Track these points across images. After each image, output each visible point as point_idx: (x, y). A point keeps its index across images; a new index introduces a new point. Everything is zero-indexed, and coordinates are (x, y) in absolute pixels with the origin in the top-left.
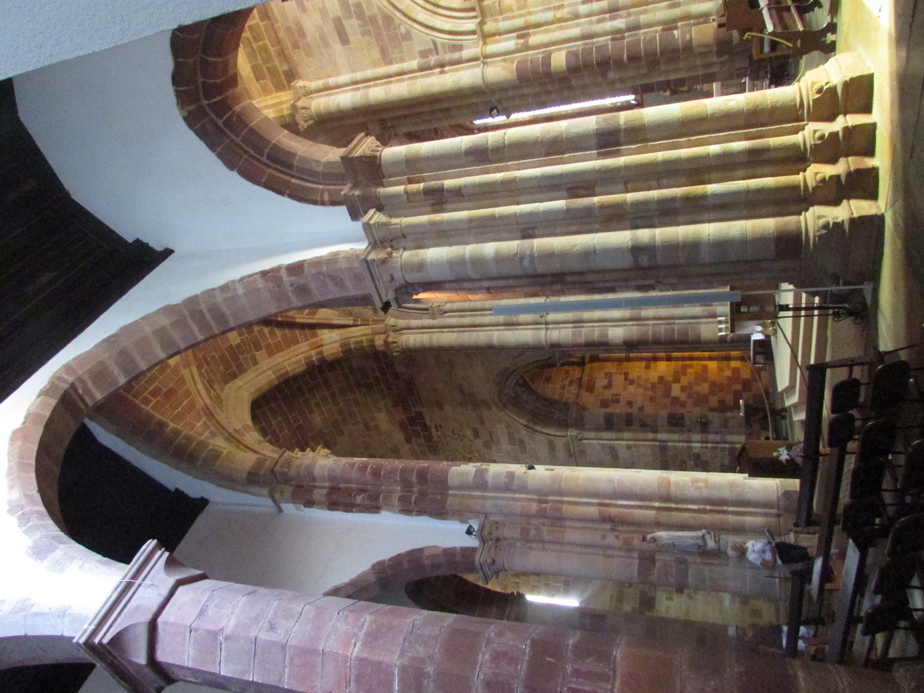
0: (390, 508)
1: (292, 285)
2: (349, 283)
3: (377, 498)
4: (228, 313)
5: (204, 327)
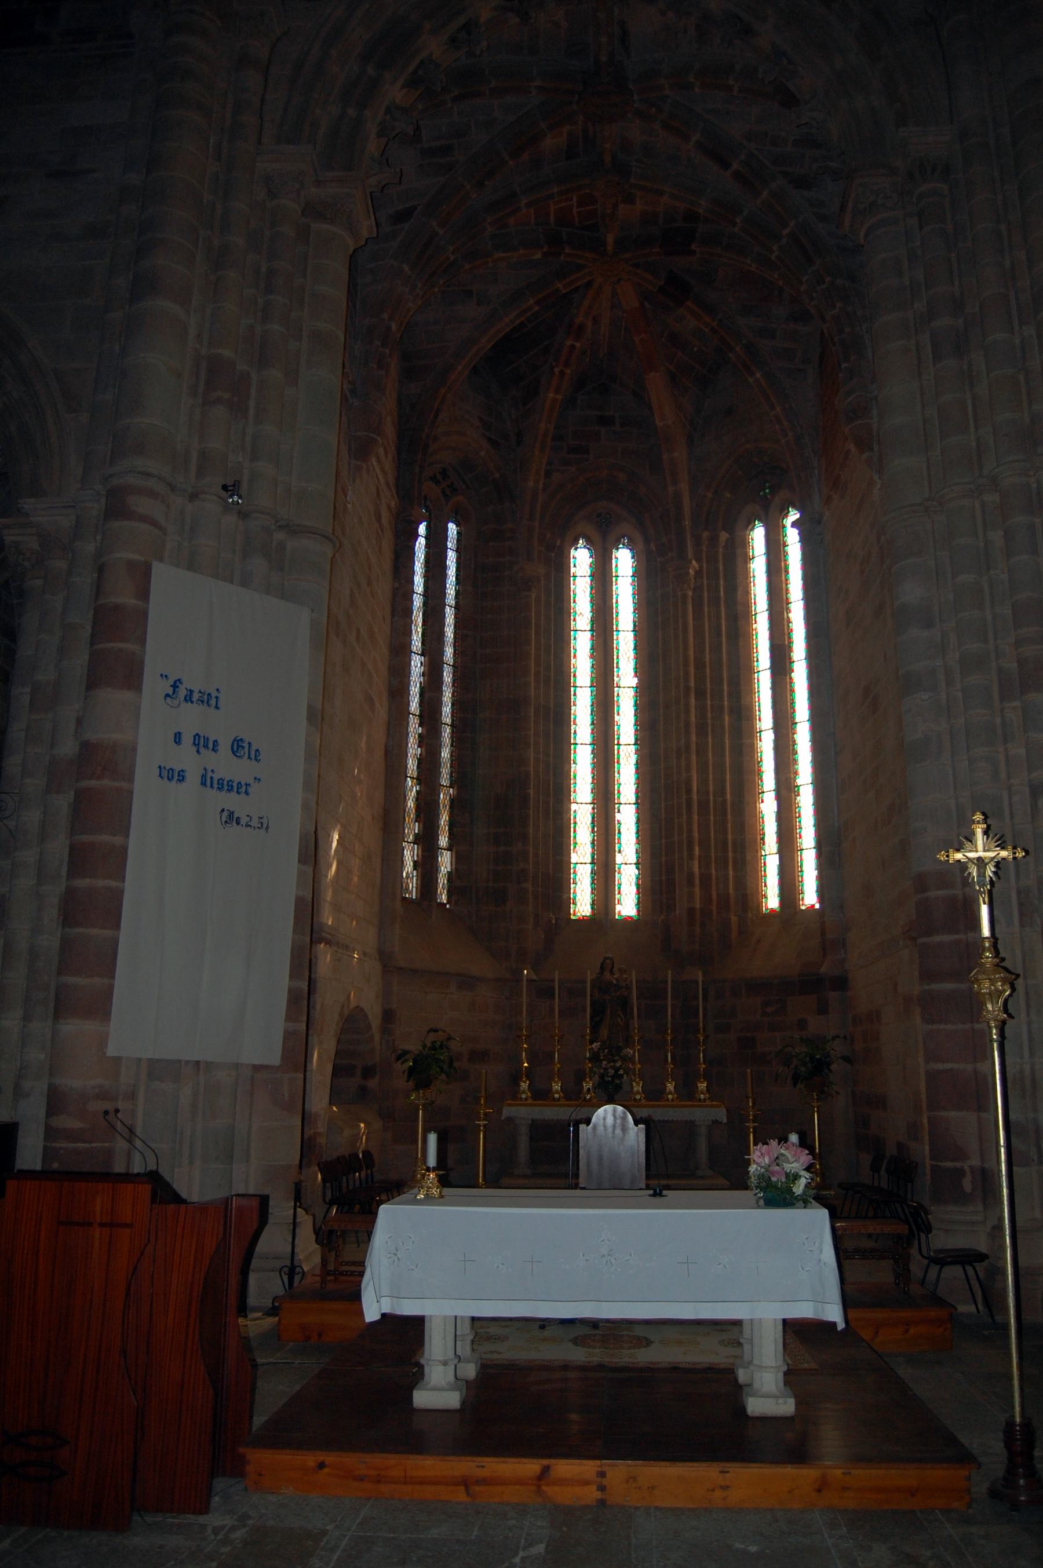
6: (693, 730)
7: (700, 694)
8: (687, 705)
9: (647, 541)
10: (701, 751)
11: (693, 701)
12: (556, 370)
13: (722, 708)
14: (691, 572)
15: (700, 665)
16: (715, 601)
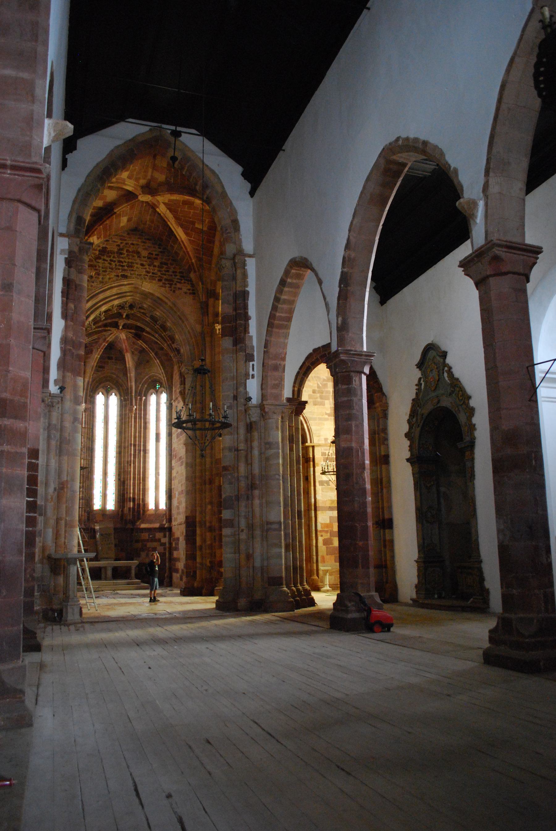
0: (66, 327)
1: (280, 364)
2: (274, 391)
3: (72, 320)
4: (280, 331)
5: (281, 319)
6: (132, 456)
7: (135, 445)
8: (131, 449)
9: (121, 396)
10: (134, 463)
11: (132, 448)
12: (99, 350)
13: (141, 449)
14: (134, 409)
15: (135, 437)
16: (140, 418)
